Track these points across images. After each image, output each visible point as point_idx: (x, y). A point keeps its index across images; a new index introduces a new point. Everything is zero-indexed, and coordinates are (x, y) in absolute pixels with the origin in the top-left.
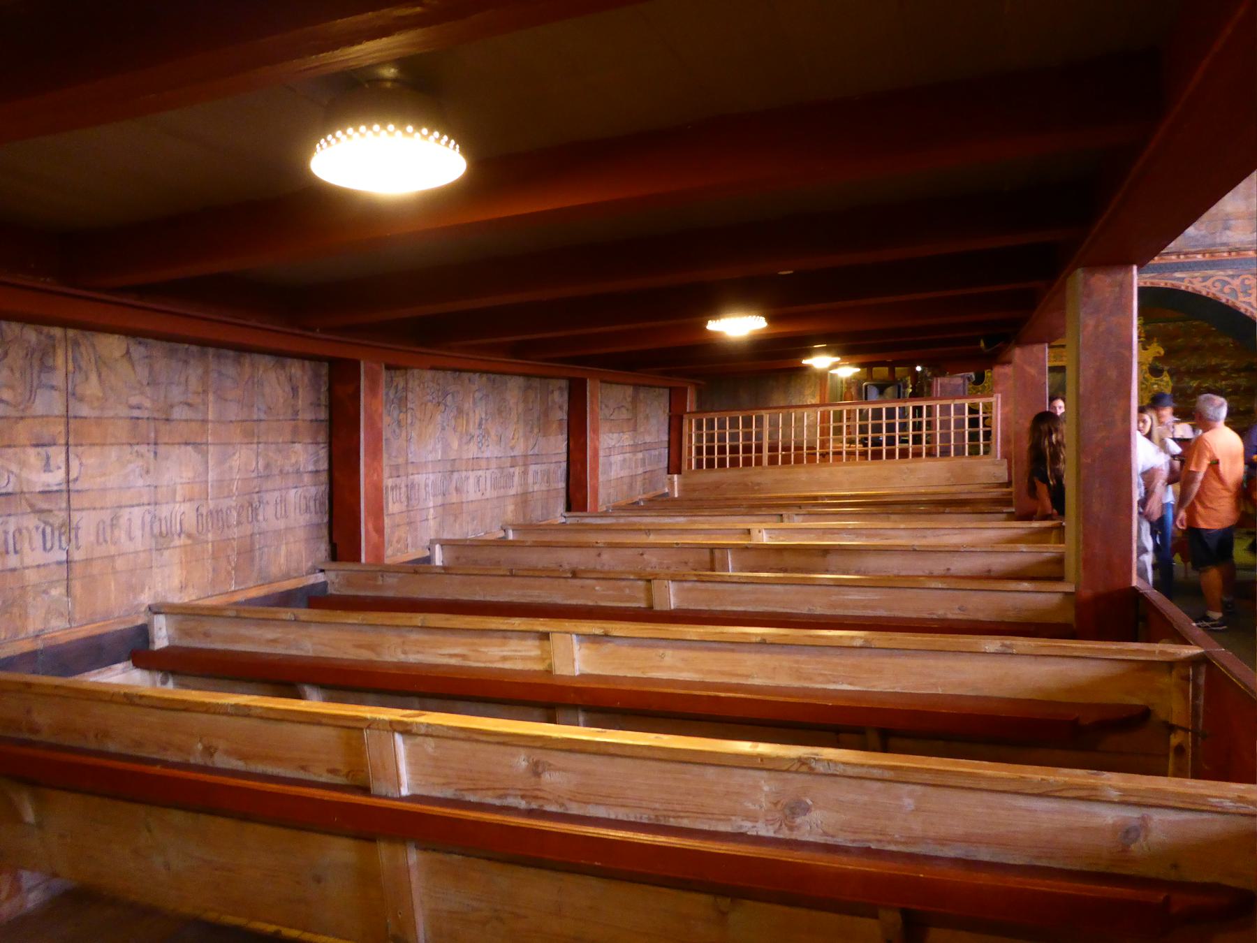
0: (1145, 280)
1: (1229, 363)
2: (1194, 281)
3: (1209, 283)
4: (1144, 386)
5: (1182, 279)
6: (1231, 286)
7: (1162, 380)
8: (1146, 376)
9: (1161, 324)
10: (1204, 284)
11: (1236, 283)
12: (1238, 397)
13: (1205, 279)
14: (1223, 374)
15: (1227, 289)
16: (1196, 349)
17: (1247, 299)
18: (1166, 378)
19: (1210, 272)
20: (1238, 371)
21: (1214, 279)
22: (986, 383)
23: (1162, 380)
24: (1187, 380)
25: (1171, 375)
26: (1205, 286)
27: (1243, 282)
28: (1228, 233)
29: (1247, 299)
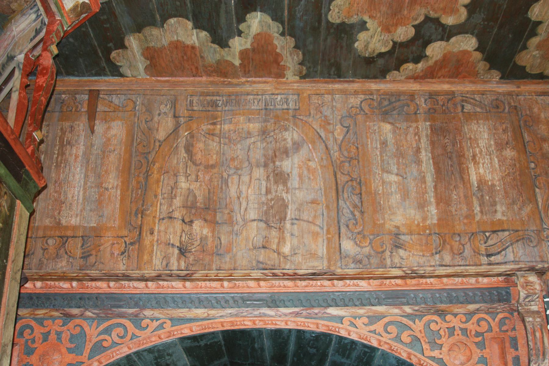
0: (286, 318)
2: (359, 322)
3: (379, 327)
5: (341, 319)
6: (412, 333)
10: (372, 328)
11: (418, 326)
13: (373, 319)
15: (405, 337)
17: (436, 353)
21: (386, 320)
26: (374, 332)
27: (427, 325)
28: (401, 252)
29: (436, 353)
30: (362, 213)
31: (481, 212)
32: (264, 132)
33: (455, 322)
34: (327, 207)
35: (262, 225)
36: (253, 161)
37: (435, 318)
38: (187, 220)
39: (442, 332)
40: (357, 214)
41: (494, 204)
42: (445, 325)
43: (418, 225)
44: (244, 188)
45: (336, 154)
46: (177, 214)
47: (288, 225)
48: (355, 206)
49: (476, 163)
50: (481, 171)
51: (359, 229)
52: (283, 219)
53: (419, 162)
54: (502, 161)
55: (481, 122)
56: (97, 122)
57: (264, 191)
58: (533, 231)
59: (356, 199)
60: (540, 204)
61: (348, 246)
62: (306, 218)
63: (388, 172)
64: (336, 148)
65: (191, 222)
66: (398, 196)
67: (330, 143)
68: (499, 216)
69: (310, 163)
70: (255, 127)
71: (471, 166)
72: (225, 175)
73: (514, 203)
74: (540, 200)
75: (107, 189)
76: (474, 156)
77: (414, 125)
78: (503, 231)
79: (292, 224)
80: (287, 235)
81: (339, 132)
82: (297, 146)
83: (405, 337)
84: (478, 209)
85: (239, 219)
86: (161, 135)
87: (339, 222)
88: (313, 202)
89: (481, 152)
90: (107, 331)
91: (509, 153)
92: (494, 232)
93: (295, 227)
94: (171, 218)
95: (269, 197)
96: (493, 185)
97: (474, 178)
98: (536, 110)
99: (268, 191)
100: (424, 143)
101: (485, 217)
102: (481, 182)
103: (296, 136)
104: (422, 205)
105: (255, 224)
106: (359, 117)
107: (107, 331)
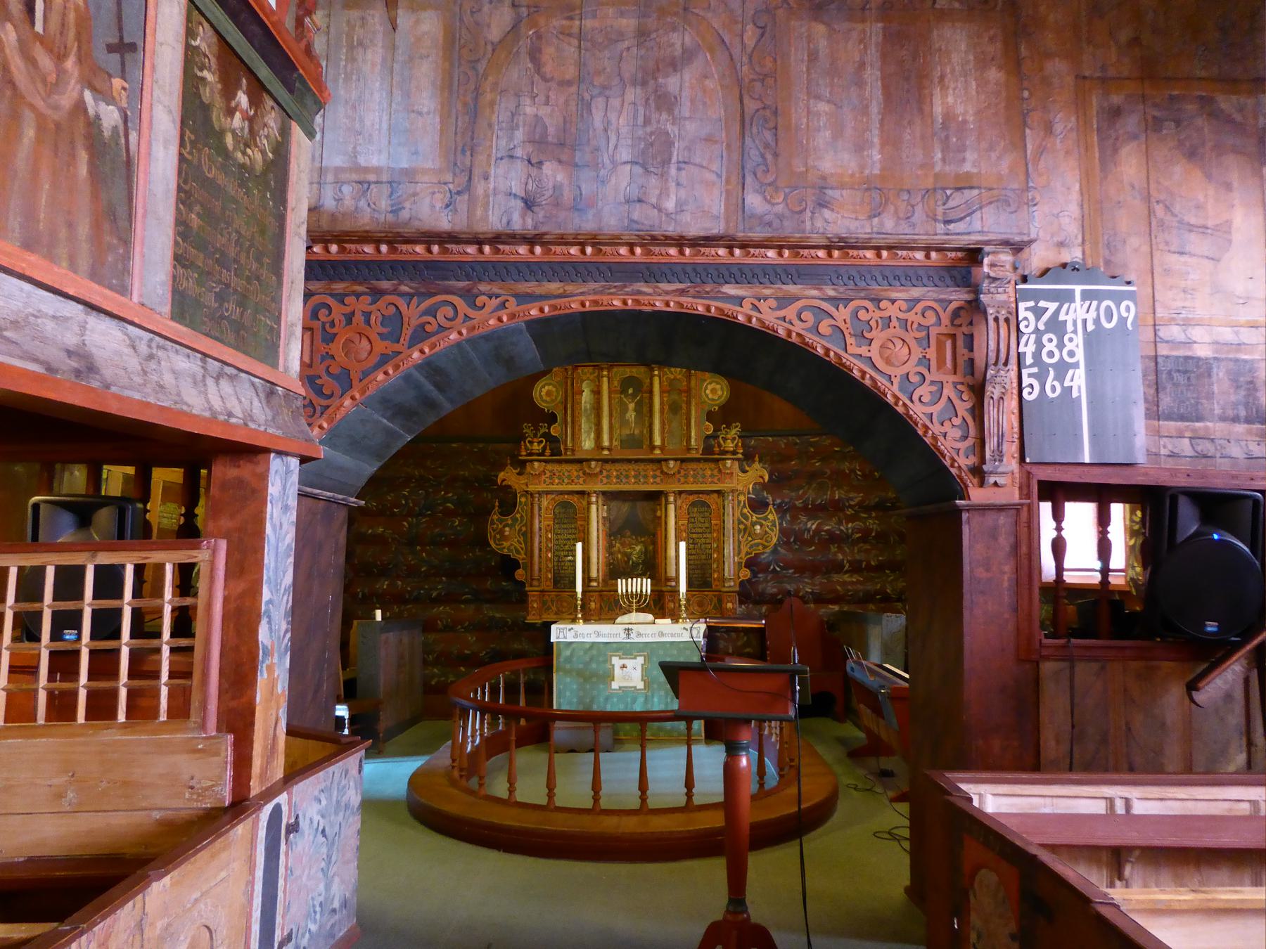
0: (667, 298)
1: (857, 498)
2: (763, 305)
3: (790, 312)
4: (742, 527)
5: (740, 300)
6: (833, 322)
7: (766, 519)
8: (745, 511)
9: (770, 439)
10: (781, 313)
11: (843, 314)
12: (867, 547)
13: (784, 301)
14: (849, 512)
16: (813, 476)
17: (863, 350)
18: (772, 516)
19: (792, 289)
20: (868, 509)
21: (800, 304)
22: (518, 512)
23: (766, 519)
24: (804, 519)
25: (780, 509)
26: (784, 319)
27: (855, 314)
28: (827, 213)
29: (863, 350)
30: (776, 155)
31: (944, 160)
32: (642, 34)
33: (892, 311)
34: (728, 146)
35: (638, 170)
36: (627, 75)
37: (867, 304)
38: (534, 161)
39: (873, 323)
40: (769, 157)
41: (962, 149)
42: (878, 314)
43: (852, 175)
44: (613, 116)
45: (745, 68)
46: (519, 152)
47: (673, 171)
48: (767, 146)
49: (944, 88)
50: (950, 100)
51: (770, 179)
52: (666, 162)
53: (860, 84)
54: (982, 83)
55: (958, 25)
56: (400, 12)
57: (641, 120)
58: (1014, 190)
59: (768, 136)
60: (1029, 152)
61: (754, 201)
62: (698, 160)
63: (818, 97)
64: (745, 59)
65: (541, 163)
66: (828, 133)
67: (736, 51)
68: (967, 167)
69: (707, 82)
70: (628, 23)
71: (937, 92)
72: (587, 97)
73: (991, 148)
74: (1029, 147)
75: (420, 113)
76: (942, 78)
77: (860, 26)
78: (971, 188)
79: (679, 169)
80: (672, 185)
81: (750, 35)
82: (688, 56)
83: (824, 327)
84: (939, 155)
85: (607, 161)
86: (495, 34)
87: (743, 168)
88: (709, 139)
89: (953, 71)
90: (432, 312)
91: (994, 74)
92: (958, 189)
93: (683, 173)
94: (511, 157)
95: (648, 129)
96: (965, 122)
97: (938, 110)
98: (1042, 9)
99: (647, 121)
100: (873, 54)
101: (947, 168)
102: (948, 117)
103: (687, 39)
104: (860, 147)
105: (628, 167)
106: (780, 12)
107: (432, 312)
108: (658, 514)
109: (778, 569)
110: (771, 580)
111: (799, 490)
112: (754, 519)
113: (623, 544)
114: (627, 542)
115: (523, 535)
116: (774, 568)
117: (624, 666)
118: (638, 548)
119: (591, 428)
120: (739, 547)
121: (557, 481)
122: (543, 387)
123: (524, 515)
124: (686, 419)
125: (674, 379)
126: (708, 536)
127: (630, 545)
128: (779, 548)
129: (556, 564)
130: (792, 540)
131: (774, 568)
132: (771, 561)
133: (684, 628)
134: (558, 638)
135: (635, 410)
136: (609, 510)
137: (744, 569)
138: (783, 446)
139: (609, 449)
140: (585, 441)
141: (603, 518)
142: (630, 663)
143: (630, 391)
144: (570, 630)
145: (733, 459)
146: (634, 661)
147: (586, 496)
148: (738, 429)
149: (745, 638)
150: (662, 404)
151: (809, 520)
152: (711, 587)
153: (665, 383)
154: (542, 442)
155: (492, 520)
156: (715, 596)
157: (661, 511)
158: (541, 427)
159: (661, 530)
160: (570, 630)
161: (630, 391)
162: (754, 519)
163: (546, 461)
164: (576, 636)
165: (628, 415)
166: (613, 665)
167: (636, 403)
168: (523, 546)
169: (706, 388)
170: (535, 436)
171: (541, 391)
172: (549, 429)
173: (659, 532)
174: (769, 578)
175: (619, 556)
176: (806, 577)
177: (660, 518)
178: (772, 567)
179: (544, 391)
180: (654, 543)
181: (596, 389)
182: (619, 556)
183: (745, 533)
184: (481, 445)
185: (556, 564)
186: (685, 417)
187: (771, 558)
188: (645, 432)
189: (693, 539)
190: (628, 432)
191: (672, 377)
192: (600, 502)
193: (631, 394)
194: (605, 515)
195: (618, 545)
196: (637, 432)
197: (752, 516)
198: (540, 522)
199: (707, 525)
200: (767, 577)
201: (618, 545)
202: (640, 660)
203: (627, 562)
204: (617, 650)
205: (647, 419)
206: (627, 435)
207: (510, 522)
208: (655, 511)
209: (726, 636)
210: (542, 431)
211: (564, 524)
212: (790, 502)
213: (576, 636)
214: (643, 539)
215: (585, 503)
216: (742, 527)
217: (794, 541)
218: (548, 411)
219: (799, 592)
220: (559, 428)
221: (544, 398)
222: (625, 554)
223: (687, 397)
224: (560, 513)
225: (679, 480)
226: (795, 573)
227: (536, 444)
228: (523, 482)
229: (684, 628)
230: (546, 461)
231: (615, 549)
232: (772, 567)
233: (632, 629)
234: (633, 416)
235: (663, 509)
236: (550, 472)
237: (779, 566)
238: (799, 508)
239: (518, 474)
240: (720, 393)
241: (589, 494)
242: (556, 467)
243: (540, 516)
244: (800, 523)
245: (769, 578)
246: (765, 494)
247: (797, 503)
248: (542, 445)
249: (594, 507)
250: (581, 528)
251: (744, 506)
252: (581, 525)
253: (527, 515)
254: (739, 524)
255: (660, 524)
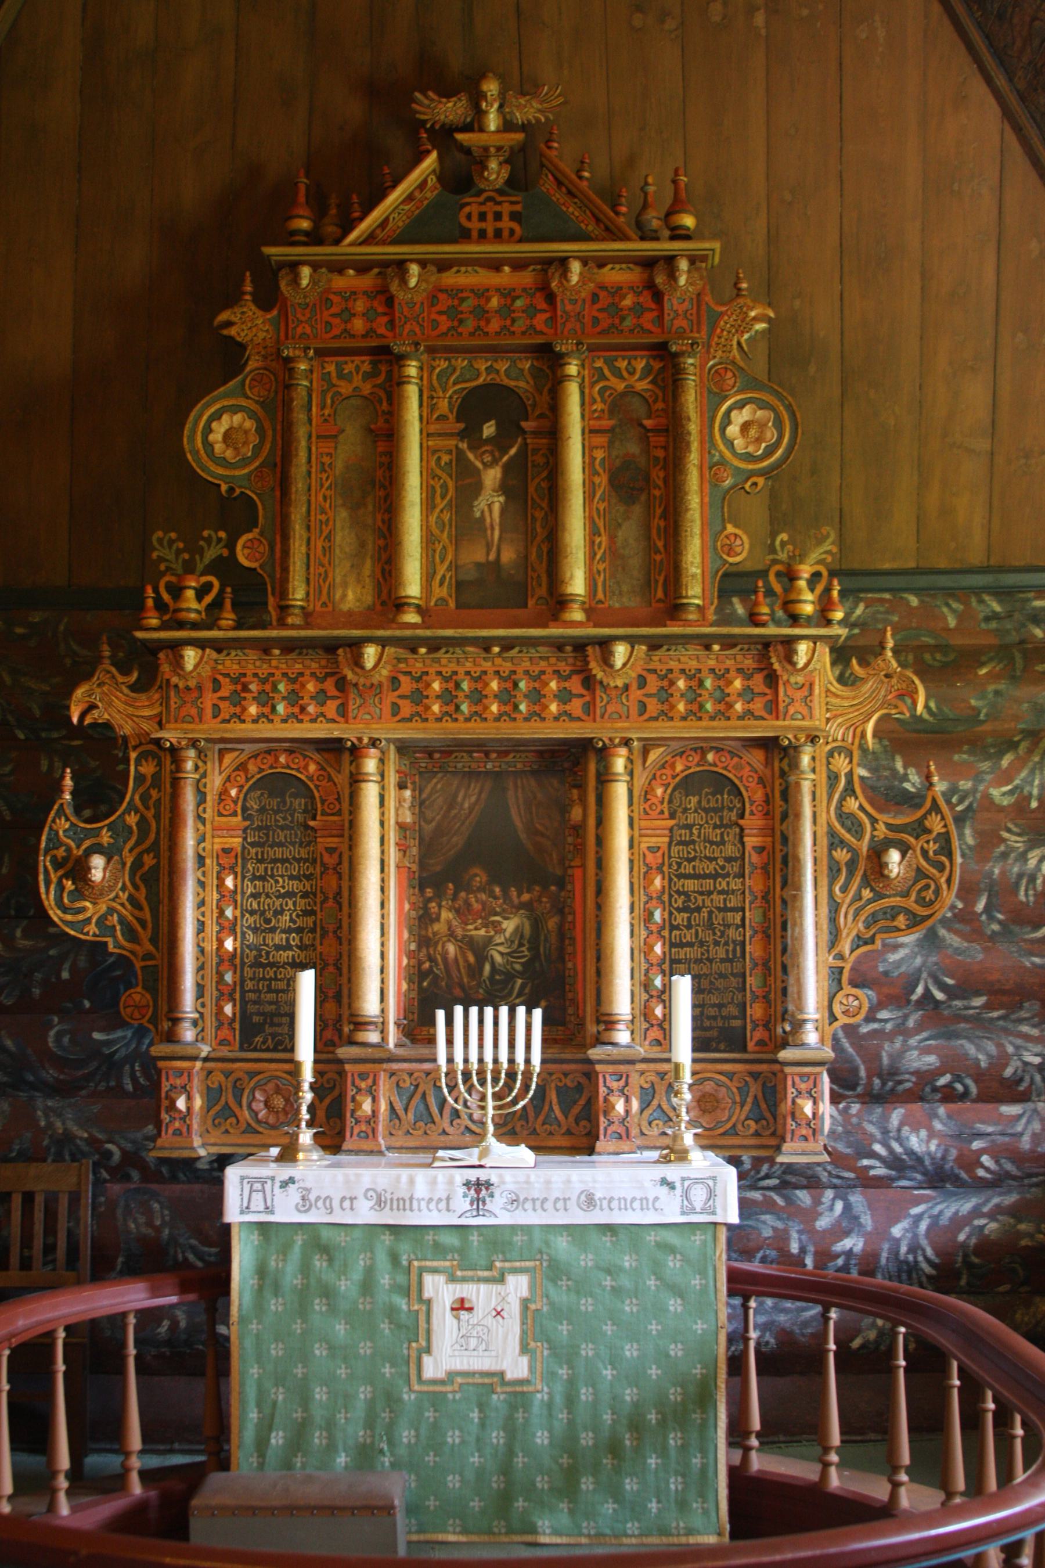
108: (576, 813)
109: (939, 996)
110: (919, 1028)
111: (1001, 754)
112: (882, 830)
113: (463, 913)
114: (476, 906)
115: (144, 879)
116: (927, 994)
117: (461, 1306)
118: (510, 926)
119: (362, 545)
120: (833, 920)
121: (253, 710)
122: (217, 416)
123: (150, 814)
124: (665, 516)
125: (624, 394)
126: (735, 884)
127: (486, 915)
128: (942, 932)
129: (248, 972)
130: (980, 906)
131: (927, 994)
132: (919, 971)
133: (664, 1182)
134: (246, 1210)
135: (504, 488)
136: (420, 805)
137: (848, 989)
138: (952, 622)
139: (419, 609)
140: (345, 585)
141: (401, 826)
142: (480, 1294)
143: (489, 430)
144: (284, 1184)
145: (815, 639)
146: (495, 1288)
147: (346, 757)
148: (827, 546)
149: (839, 1206)
150: (589, 467)
151: (1032, 845)
152: (744, 1049)
153: (599, 406)
154: (208, 586)
155: (54, 833)
156: (755, 1075)
157: (583, 801)
158: (209, 540)
159: (583, 866)
160: (284, 1184)
161: (489, 430)
162: (882, 830)
163: (219, 646)
164: (305, 1203)
165: (481, 504)
166: (429, 1302)
167: (507, 469)
168: (147, 915)
169: (727, 421)
170: (189, 568)
171: (208, 430)
172: (231, 546)
173: (577, 873)
174: (911, 1023)
175: (451, 948)
176: (1020, 1021)
177: (578, 829)
178: (920, 990)
179: (220, 429)
180: (561, 909)
181: (381, 423)
182: (451, 948)
183: (851, 874)
184: (36, 617)
185: (248, 972)
186: (659, 511)
187: (918, 961)
188: (533, 556)
189: (686, 894)
190: (479, 556)
191: (621, 386)
192: (392, 778)
193: (489, 440)
194: (408, 818)
195: (445, 915)
196: (508, 555)
197: (874, 821)
198: (201, 839)
199: (730, 850)
200: (906, 1017)
201: (445, 915)
202: (518, 1286)
203: (475, 971)
204: (440, 1250)
205: (539, 514)
206: (478, 565)
207: (106, 838)
208: (564, 809)
209: (780, 1201)
210: (211, 554)
211: (280, 845)
212: (974, 790)
213: (305, 1203)
214: (526, 897)
215: (342, 779)
216: (842, 855)
217: (987, 909)
218: (231, 490)
219: (1006, 1065)
220: (264, 548)
221: (218, 448)
222: (469, 943)
223: (665, 448)
224: (262, 810)
225: (643, 707)
226: (988, 1006)
227: (190, 594)
228: (147, 713)
229: (664, 1182)
230: (219, 646)
231: (440, 927)
232: (920, 990)
233: (488, 1185)
234: (496, 508)
235: (592, 799)
236: (235, 681)
237: (943, 987)
238: (1001, 809)
239: (133, 688)
240: (771, 435)
241: (356, 752)
242: (251, 662)
243: (200, 818)
244: (1004, 855)
245: (911, 1023)
246: (899, 765)
247: (995, 793)
248: (208, 599)
249: (370, 793)
250: (330, 860)
251: (850, 791)
252: (331, 851)
253: (157, 817)
254: (832, 846)
255: (580, 849)
